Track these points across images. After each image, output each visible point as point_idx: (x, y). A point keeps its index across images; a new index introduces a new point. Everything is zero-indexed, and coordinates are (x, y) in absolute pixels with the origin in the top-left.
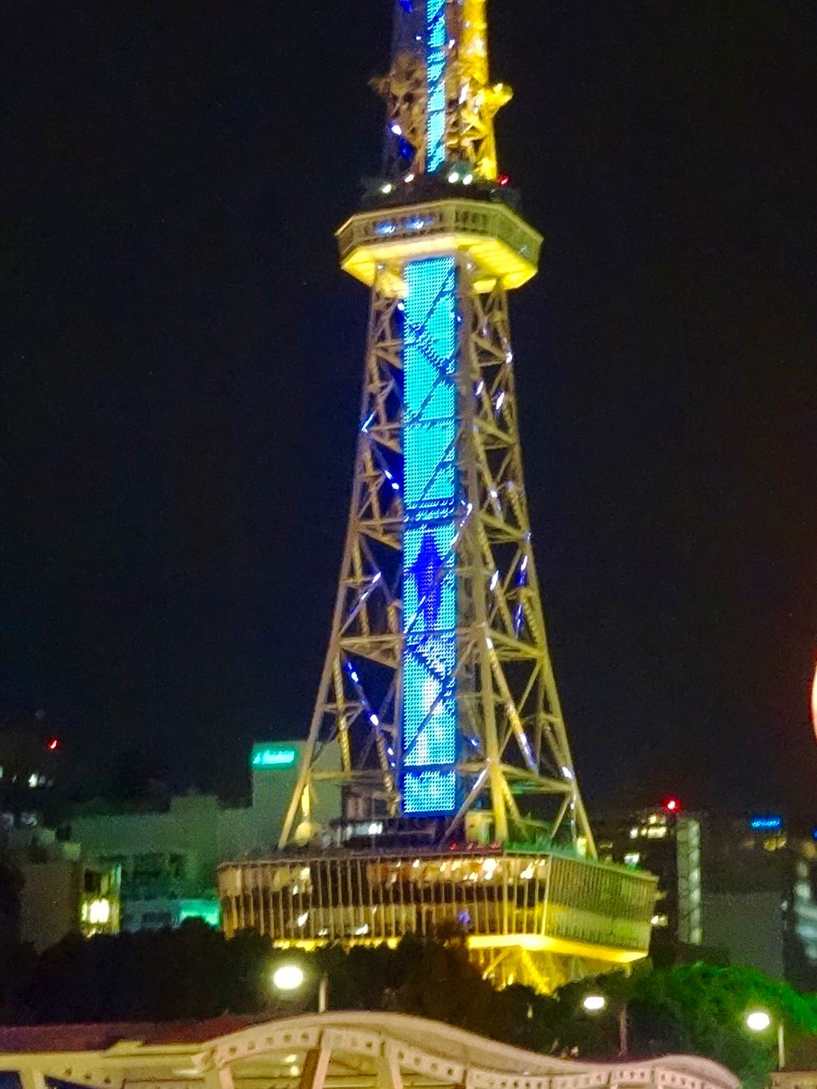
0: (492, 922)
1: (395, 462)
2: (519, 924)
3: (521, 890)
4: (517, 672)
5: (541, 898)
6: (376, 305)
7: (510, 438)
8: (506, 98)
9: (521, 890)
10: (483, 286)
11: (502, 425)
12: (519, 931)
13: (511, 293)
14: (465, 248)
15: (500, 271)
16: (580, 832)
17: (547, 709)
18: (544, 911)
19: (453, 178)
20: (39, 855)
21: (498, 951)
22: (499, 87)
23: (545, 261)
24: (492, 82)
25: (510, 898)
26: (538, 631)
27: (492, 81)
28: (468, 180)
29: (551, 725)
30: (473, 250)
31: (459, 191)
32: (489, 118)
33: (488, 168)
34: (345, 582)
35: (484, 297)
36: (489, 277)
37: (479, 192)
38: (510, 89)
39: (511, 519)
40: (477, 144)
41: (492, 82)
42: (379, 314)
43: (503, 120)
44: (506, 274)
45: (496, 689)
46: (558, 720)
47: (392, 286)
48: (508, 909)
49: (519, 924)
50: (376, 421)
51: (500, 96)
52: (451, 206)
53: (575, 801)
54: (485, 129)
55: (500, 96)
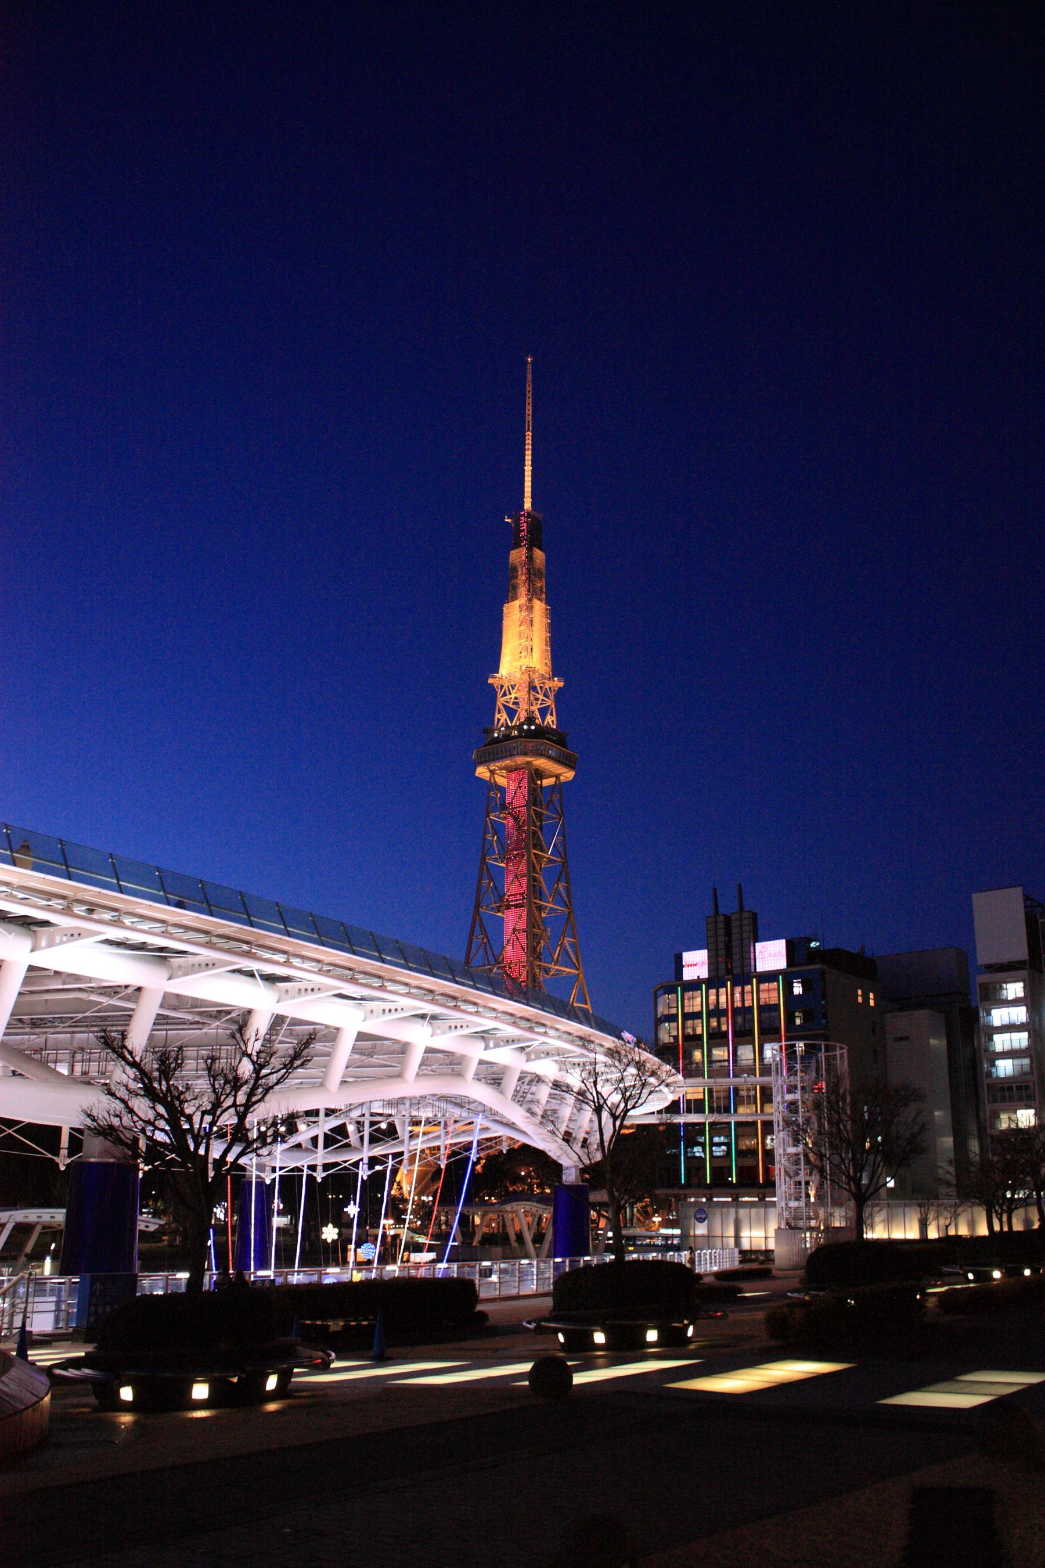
8: (561, 684)
14: (529, 763)
22: (556, 679)
24: (554, 676)
27: (554, 676)
30: (534, 762)
44: (560, 774)
51: (558, 683)
54: (550, 702)
55: (558, 683)
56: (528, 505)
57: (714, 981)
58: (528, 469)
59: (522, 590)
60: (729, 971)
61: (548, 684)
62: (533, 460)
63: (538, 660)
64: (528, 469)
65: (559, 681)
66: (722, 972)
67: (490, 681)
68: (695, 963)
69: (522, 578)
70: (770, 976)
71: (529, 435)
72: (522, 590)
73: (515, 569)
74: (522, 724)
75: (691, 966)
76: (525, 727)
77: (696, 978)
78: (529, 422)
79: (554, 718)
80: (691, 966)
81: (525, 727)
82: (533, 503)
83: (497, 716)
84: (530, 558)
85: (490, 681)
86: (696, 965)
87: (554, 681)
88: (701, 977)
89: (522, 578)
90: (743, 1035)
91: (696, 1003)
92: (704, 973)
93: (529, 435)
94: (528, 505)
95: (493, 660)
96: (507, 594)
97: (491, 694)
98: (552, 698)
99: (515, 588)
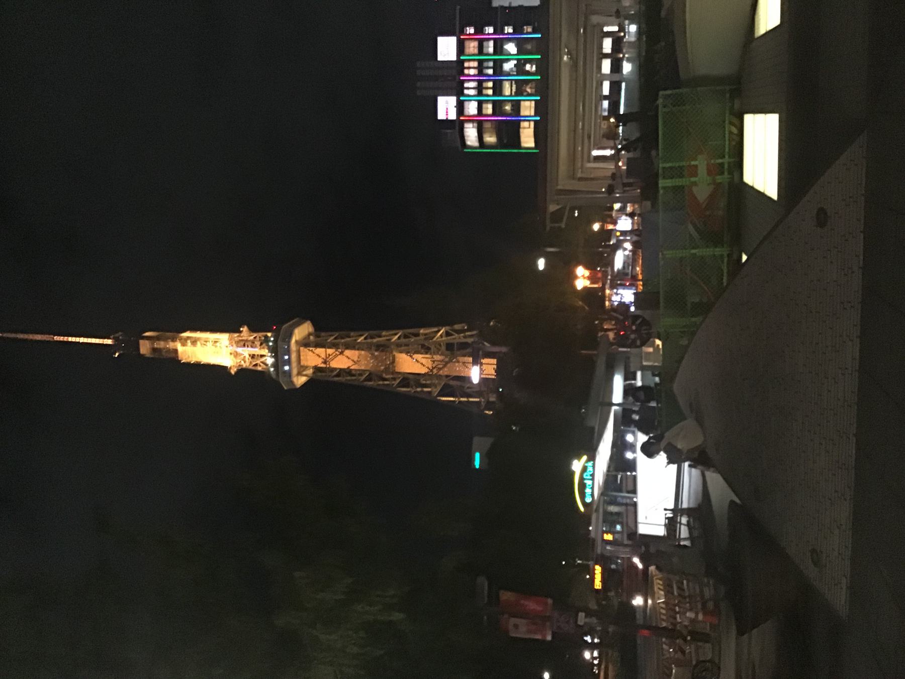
13: (316, 330)
14: (296, 341)
30: (297, 339)
32: (252, 334)
38: (243, 326)
41: (241, 332)
43: (252, 329)
51: (245, 329)
55: (245, 329)
56: (109, 342)
57: (458, 91)
58: (82, 340)
59: (171, 345)
63: (224, 338)
64: (82, 340)
65: (243, 327)
68: (446, 109)
69: (161, 345)
70: (461, 49)
71: (56, 338)
72: (171, 345)
73: (154, 350)
75: (447, 112)
76: (271, 344)
77: (455, 109)
78: (47, 337)
80: (447, 112)
81: (271, 344)
82: (109, 338)
84: (148, 338)
86: (447, 109)
87: (242, 331)
88: (456, 105)
89: (161, 345)
91: (471, 108)
92: (452, 100)
93: (56, 338)
94: (109, 342)
95: (220, 370)
96: (173, 359)
97: (242, 371)
99: (168, 350)
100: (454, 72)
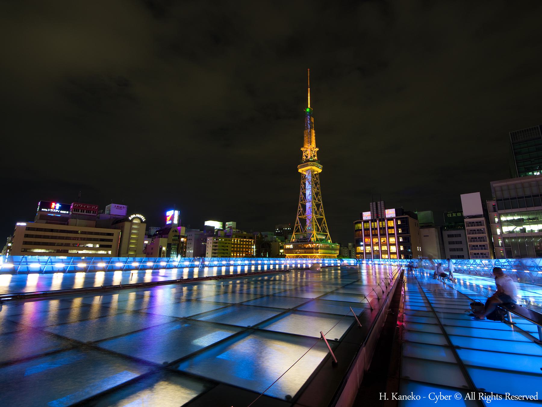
0: (313, 252)
1: (304, 194)
2: (316, 252)
3: (316, 248)
4: (320, 221)
5: (319, 249)
6: (302, 176)
7: (320, 191)
8: (318, 150)
9: (316, 248)
10: (315, 173)
11: (318, 189)
12: (316, 253)
14: (312, 168)
15: (318, 170)
16: (329, 239)
17: (325, 224)
18: (319, 251)
19: (310, 160)
20: (276, 241)
21: (314, 255)
23: (323, 169)
25: (315, 249)
26: (324, 214)
28: (312, 160)
29: (325, 226)
31: (311, 161)
32: (316, 152)
33: (316, 158)
34: (299, 209)
35: (315, 175)
36: (316, 171)
37: (314, 161)
39: (319, 201)
40: (314, 156)
42: (303, 177)
43: (318, 152)
45: (316, 222)
46: (326, 225)
47: (305, 173)
48: (314, 251)
49: (316, 252)
50: (303, 189)
51: (317, 149)
52: (309, 163)
53: (329, 234)
54: (316, 154)
55: (317, 149)
57: (373, 220)
58: (309, 97)
60: (377, 217)
61: (315, 150)
62: (310, 95)
64: (309, 97)
66: (375, 218)
67: (301, 149)
74: (309, 159)
79: (317, 158)
83: (303, 157)
85: (301, 149)
90: (383, 235)
98: (316, 153)
100: (380, 217)
